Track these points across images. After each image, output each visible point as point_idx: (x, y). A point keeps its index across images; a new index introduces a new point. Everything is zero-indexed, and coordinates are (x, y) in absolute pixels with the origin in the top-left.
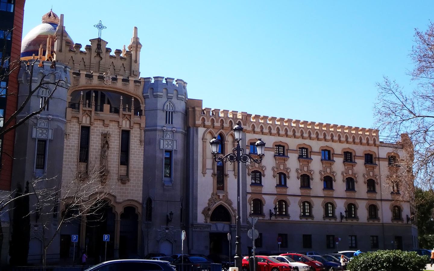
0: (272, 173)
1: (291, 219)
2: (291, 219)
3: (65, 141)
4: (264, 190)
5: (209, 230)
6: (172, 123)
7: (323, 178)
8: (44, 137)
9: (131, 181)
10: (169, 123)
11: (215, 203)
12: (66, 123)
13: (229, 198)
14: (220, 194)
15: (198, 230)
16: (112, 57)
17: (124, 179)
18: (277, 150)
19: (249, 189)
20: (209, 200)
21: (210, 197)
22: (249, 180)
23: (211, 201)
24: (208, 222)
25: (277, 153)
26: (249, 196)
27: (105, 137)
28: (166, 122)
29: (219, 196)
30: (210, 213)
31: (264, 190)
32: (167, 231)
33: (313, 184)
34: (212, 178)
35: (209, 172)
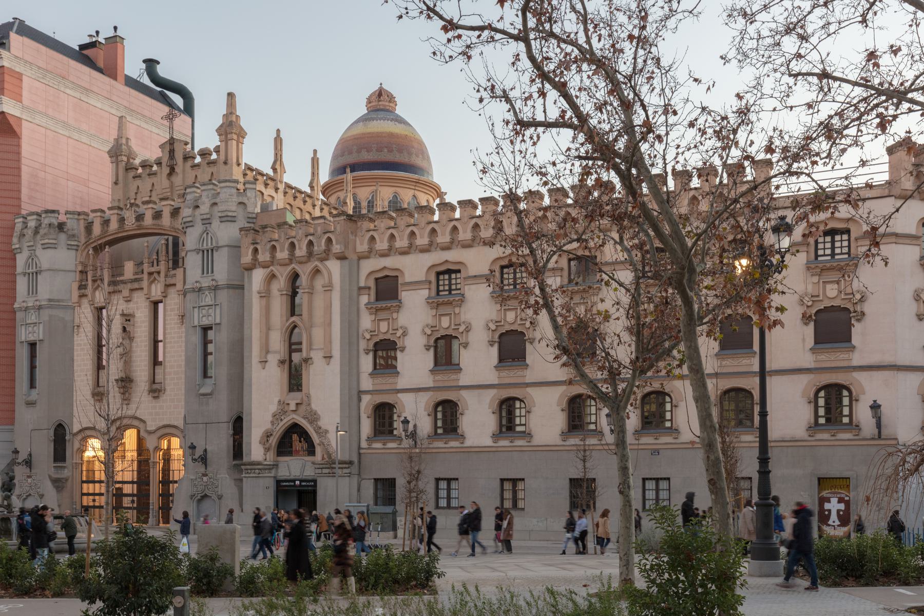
0: (423, 340)
1: (468, 443)
2: (468, 443)
3: (76, 338)
4: (403, 382)
5: (272, 475)
6: (212, 272)
7: (496, 338)
8: (32, 338)
9: (168, 392)
10: (208, 273)
11: (281, 420)
12: (74, 308)
13: (314, 406)
14: (290, 402)
15: (251, 475)
16: (195, 166)
17: (156, 390)
18: (453, 282)
19: (367, 383)
20: (274, 416)
21: (273, 408)
22: (367, 363)
23: (277, 417)
24: (268, 459)
25: (446, 290)
26: (366, 399)
27: (128, 317)
28: (203, 273)
29: (297, 404)
30: (274, 441)
31: (403, 382)
32: (205, 479)
33: (403, 361)
34: (279, 369)
35: (273, 359)
